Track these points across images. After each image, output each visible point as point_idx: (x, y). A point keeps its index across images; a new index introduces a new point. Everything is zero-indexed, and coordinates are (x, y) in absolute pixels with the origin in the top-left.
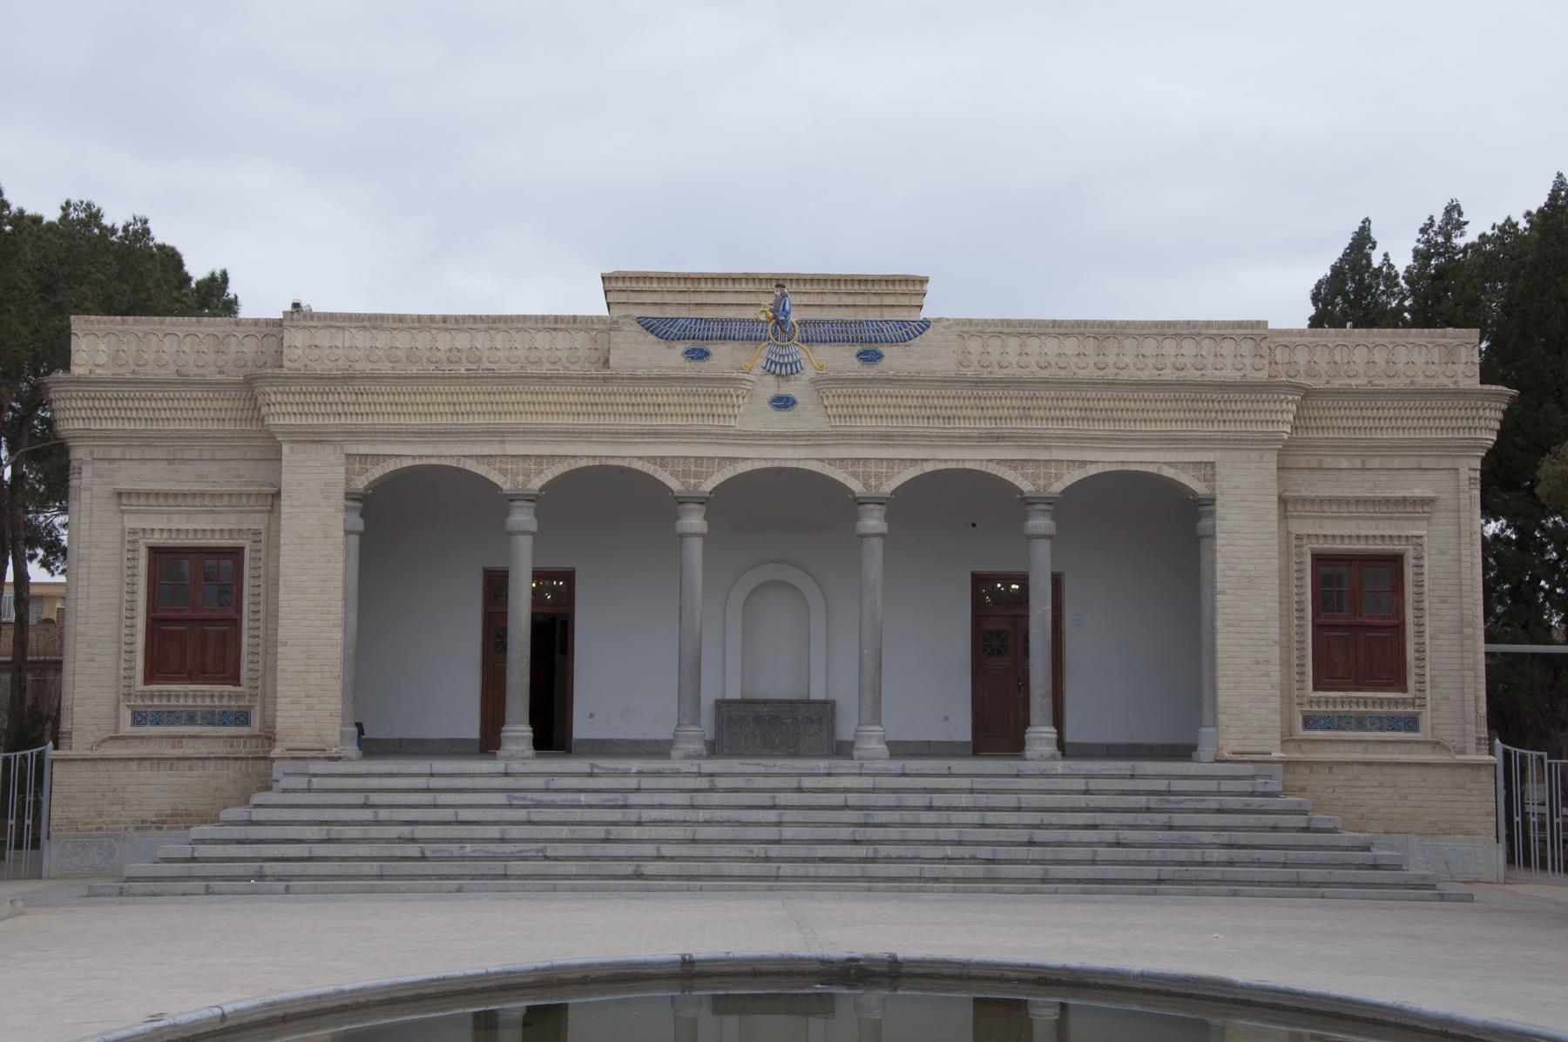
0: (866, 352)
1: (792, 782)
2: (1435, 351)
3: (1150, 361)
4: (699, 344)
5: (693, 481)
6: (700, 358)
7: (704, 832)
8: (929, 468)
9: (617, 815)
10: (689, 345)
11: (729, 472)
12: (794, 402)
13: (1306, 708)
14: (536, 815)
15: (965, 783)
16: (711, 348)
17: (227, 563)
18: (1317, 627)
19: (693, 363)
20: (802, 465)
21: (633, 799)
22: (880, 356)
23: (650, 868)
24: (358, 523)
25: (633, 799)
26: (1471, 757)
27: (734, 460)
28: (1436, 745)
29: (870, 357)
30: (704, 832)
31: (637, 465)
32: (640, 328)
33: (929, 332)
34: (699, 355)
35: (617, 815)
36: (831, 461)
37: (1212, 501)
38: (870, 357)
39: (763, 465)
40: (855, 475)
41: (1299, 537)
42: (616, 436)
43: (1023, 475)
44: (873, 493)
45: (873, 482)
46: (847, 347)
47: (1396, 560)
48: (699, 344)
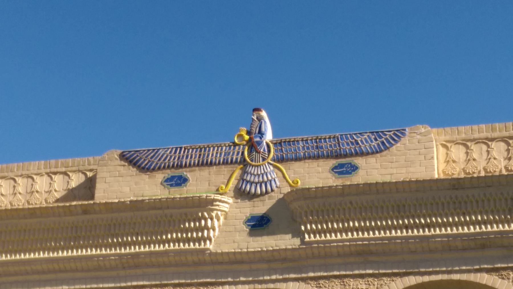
0: (341, 166)
6: (178, 185)
16: (189, 175)
19: (173, 189)
22: (354, 168)
29: (345, 170)
33: (405, 140)
38: (345, 170)
46: (321, 162)
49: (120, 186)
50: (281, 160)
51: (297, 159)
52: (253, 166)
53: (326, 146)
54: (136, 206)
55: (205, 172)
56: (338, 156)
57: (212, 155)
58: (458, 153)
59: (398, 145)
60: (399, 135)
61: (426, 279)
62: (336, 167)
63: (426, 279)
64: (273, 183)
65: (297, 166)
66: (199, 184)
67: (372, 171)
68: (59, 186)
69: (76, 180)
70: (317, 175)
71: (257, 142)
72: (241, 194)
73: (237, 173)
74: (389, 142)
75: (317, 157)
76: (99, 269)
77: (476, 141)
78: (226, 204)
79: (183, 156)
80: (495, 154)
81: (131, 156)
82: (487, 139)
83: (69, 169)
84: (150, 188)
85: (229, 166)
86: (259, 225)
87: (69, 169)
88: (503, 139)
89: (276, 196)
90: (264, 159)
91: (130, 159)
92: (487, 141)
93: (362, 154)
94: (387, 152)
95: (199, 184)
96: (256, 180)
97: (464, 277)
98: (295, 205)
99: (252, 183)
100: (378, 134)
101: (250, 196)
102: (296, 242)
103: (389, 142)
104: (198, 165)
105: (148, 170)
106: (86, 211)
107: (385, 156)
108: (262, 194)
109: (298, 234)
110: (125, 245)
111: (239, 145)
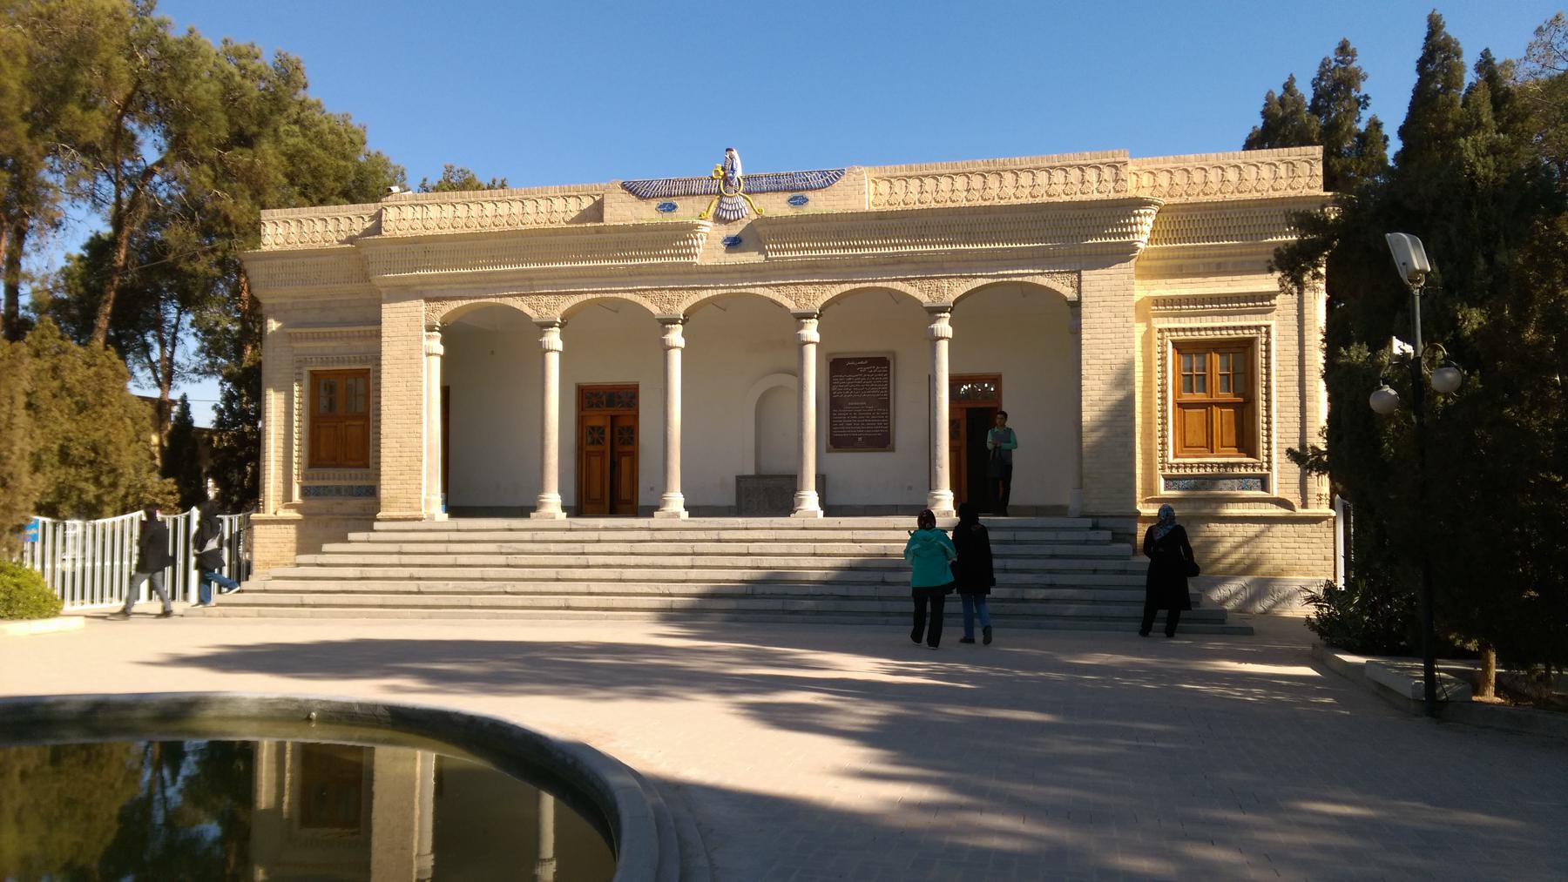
1: (714, 535)
2: (1283, 167)
3: (1027, 191)
4: (668, 200)
7: (628, 574)
9: (572, 560)
13: (1168, 472)
14: (512, 560)
15: (847, 535)
17: (361, 381)
18: (1181, 406)
21: (589, 548)
23: (575, 601)
24: (440, 349)
25: (589, 548)
26: (1312, 511)
28: (1281, 502)
29: (799, 201)
30: (628, 574)
33: (844, 178)
34: (672, 208)
35: (572, 560)
37: (1076, 305)
38: (799, 201)
41: (1160, 331)
46: (780, 195)
47: (1249, 344)
48: (668, 200)
49: (623, 211)
50: (749, 192)
51: (762, 192)
53: (784, 182)
54: (638, 228)
55: (690, 201)
56: (793, 190)
58: (884, 187)
60: (839, 174)
61: (858, 286)
63: (858, 286)
65: (761, 197)
66: (686, 211)
67: (820, 203)
68: (574, 208)
69: (587, 203)
70: (776, 206)
72: (719, 219)
73: (716, 202)
75: (777, 191)
76: (610, 276)
77: (898, 178)
78: (708, 228)
80: (911, 188)
84: (647, 213)
86: (734, 244)
88: (918, 177)
89: (746, 221)
91: (630, 188)
92: (906, 178)
93: (811, 189)
95: (686, 211)
97: (885, 285)
98: (760, 230)
100: (824, 173)
101: (726, 221)
102: (762, 257)
106: (598, 231)
109: (763, 251)
110: (631, 258)
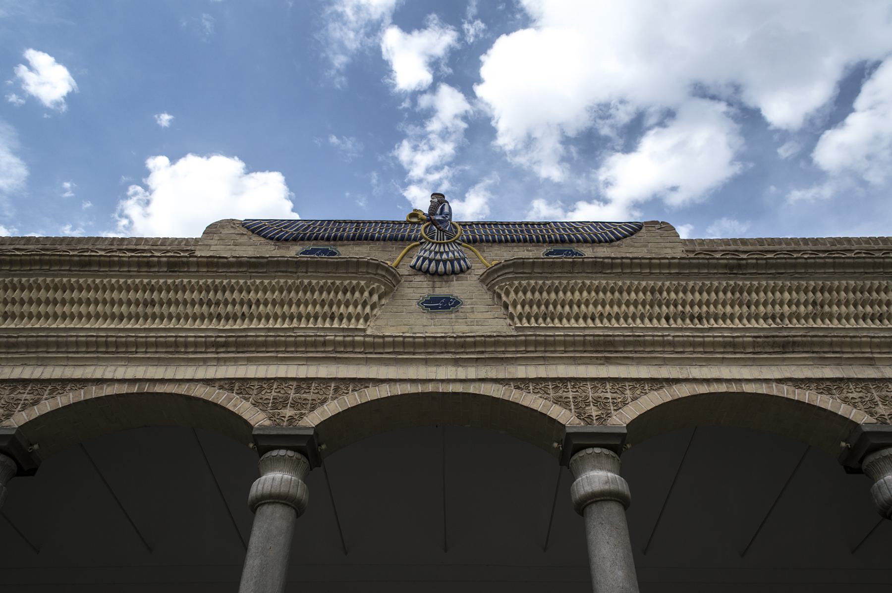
5: (289, 412)
8: (684, 391)
10: (310, 245)
11: (352, 399)
12: (457, 303)
20: (472, 389)
27: (364, 382)
31: (199, 392)
32: (244, 231)
36: (522, 383)
39: (409, 389)
40: (557, 401)
42: (175, 349)
43: (845, 400)
44: (596, 427)
45: (594, 411)
48: (322, 245)
52: (433, 243)
57: (375, 230)
59: (634, 237)
62: (551, 253)
64: (462, 262)
71: (439, 220)
74: (620, 232)
79: (332, 229)
81: (255, 224)
82: (737, 251)
83: (155, 247)
85: (400, 243)
87: (155, 247)
90: (448, 239)
94: (618, 242)
96: (438, 257)
99: (430, 261)
103: (620, 232)
104: (353, 239)
105: (278, 240)
107: (618, 246)
108: (445, 273)
111: (414, 223)
